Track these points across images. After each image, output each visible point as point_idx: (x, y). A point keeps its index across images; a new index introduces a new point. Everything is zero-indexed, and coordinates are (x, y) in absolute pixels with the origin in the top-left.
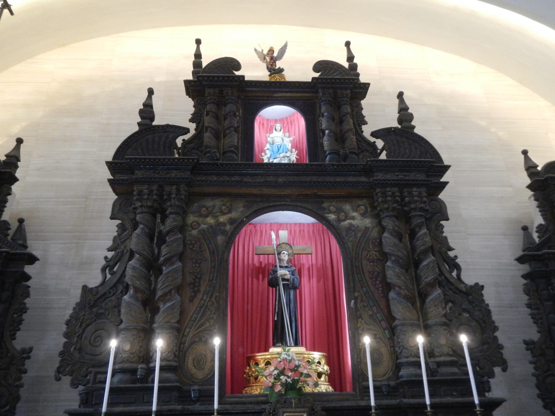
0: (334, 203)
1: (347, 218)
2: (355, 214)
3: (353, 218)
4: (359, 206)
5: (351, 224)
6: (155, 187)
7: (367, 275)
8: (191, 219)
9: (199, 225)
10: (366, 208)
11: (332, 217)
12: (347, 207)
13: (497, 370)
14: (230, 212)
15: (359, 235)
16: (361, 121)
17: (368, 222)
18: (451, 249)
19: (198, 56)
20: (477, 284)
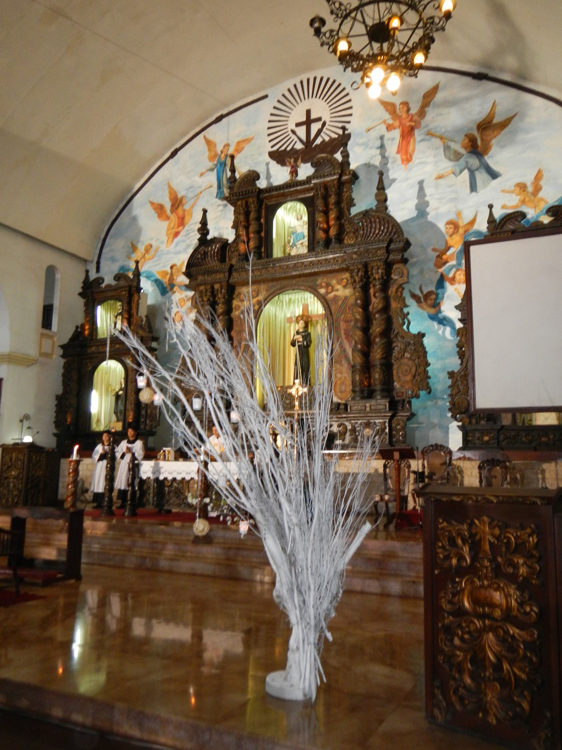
0: (325, 280)
1: (332, 291)
2: (339, 287)
3: (337, 290)
4: (343, 279)
5: (335, 296)
6: (209, 287)
7: (342, 332)
8: (235, 303)
9: (239, 307)
10: (348, 281)
11: (322, 291)
12: (334, 282)
13: (422, 393)
14: (257, 295)
15: (340, 303)
16: (351, 203)
17: (348, 292)
18: (406, 306)
19: (233, 170)
20: (419, 333)
